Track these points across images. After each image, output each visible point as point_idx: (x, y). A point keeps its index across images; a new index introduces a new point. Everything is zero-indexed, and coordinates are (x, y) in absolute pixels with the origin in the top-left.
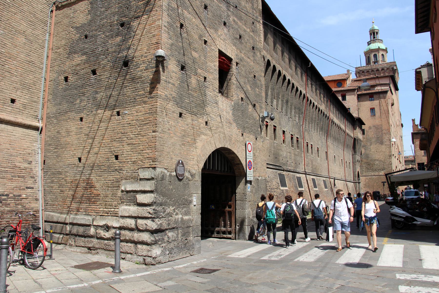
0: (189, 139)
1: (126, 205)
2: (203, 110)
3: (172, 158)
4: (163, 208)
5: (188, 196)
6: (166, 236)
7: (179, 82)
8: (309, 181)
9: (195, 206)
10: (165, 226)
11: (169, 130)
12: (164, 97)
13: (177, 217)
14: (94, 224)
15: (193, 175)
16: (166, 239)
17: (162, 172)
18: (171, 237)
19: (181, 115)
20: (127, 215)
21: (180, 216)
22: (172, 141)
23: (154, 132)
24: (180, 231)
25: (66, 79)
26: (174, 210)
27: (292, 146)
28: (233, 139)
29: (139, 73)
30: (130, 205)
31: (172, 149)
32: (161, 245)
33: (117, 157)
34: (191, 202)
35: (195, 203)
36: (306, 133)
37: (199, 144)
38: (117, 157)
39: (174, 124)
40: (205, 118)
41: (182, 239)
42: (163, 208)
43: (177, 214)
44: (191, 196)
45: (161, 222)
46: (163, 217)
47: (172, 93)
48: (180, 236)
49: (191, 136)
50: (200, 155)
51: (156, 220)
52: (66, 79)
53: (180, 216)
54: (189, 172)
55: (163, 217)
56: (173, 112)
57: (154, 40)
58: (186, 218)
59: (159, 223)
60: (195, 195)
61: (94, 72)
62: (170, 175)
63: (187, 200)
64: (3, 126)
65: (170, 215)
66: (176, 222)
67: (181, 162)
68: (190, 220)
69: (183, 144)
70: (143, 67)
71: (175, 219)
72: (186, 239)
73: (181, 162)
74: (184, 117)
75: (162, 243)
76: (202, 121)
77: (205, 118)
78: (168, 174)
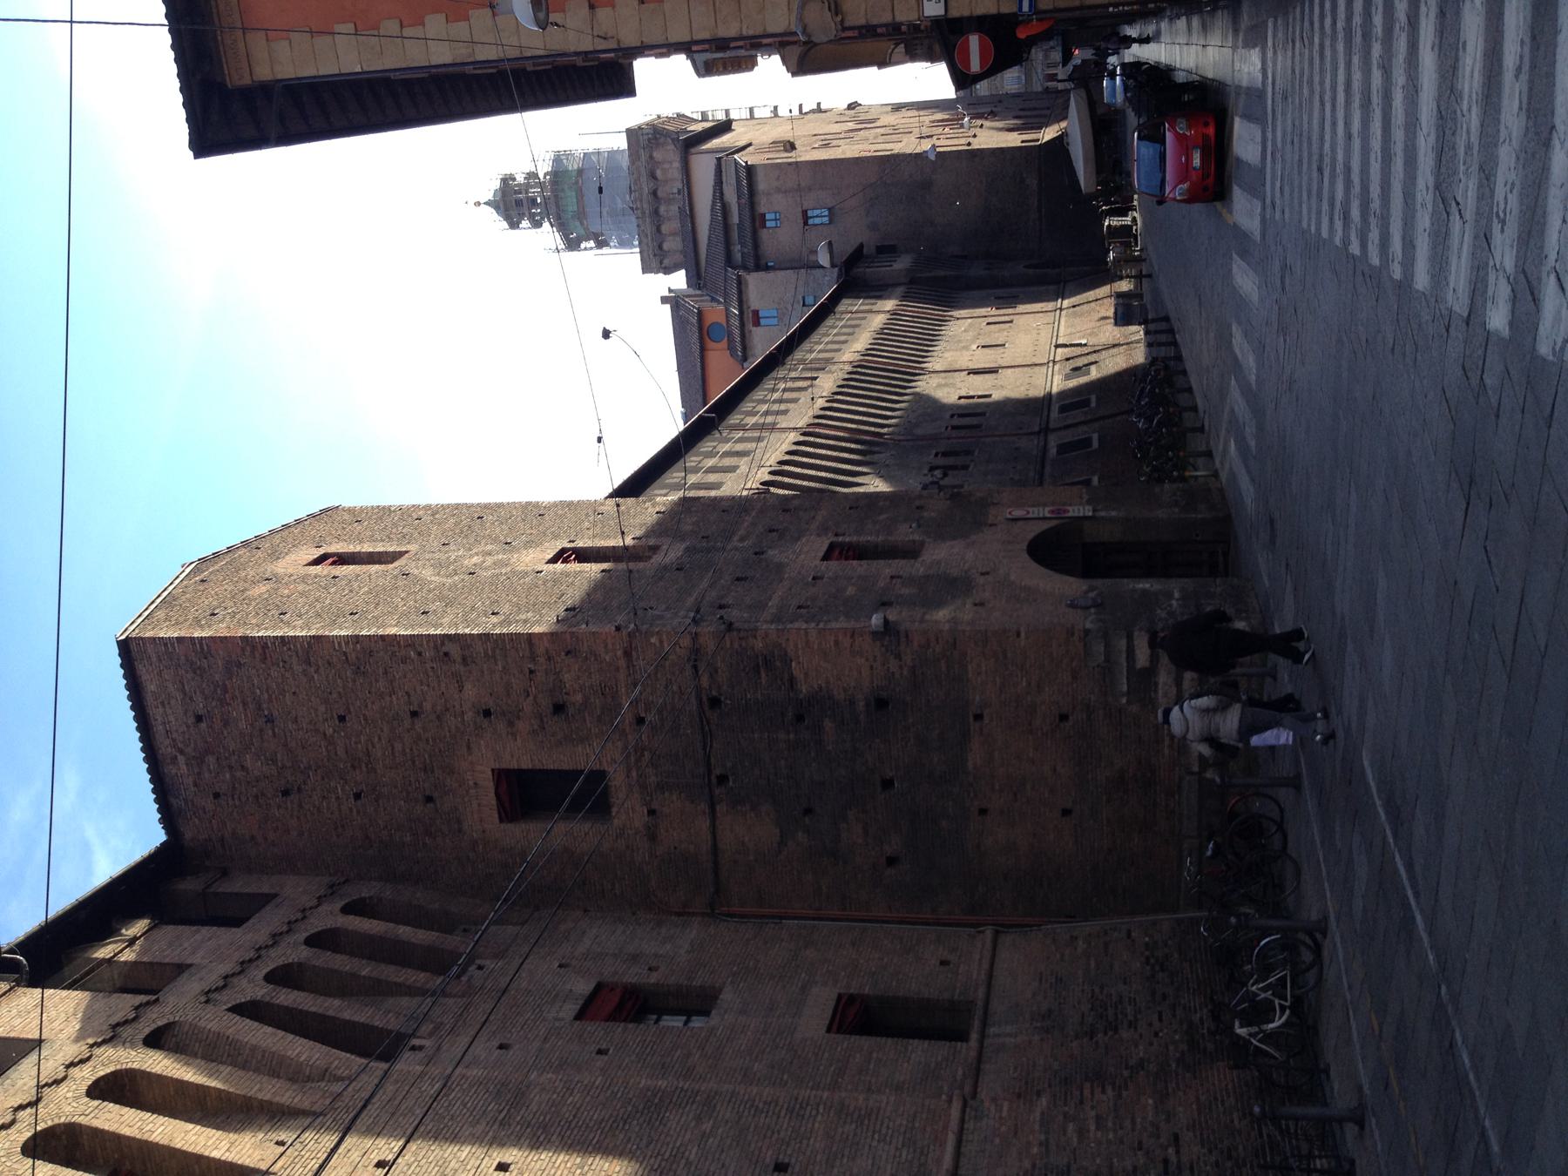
1: (1156, 691)
8: (1070, 422)
14: (1196, 769)
15: (1091, 589)
20: (1174, 690)
23: (1018, 635)
25: (891, 861)
27: (965, 467)
29: (905, 672)
30: (1156, 684)
33: (1064, 717)
36: (919, 432)
38: (1064, 717)
52: (891, 861)
57: (846, 642)
58: (1177, 595)
61: (887, 784)
64: (962, 1172)
70: (893, 665)
76: (981, 580)
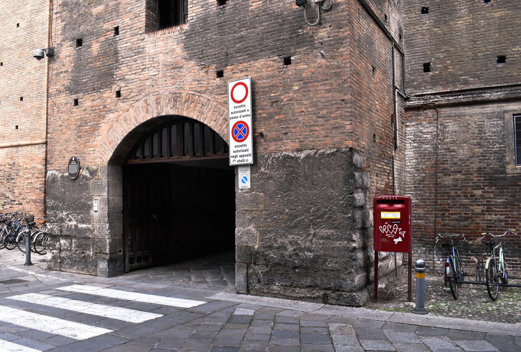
0: (87, 127)
2: (113, 77)
3: (64, 157)
4: (55, 212)
5: (86, 199)
6: (58, 243)
9: (96, 211)
10: (56, 231)
12: (55, 93)
13: (70, 223)
15: (93, 173)
16: (57, 245)
17: (52, 174)
18: (63, 244)
19: (76, 102)
21: (74, 223)
22: (64, 138)
24: (73, 240)
26: (67, 215)
28: (184, 95)
31: (64, 146)
32: (53, 251)
34: (90, 207)
37: (104, 127)
40: (115, 88)
41: (77, 250)
42: (55, 212)
43: (70, 220)
44: (91, 200)
45: (52, 226)
46: (54, 222)
48: (73, 245)
50: (105, 143)
53: (74, 223)
54: (87, 169)
56: (67, 103)
58: (80, 226)
59: (49, 227)
60: (98, 198)
62: (62, 177)
63: (84, 205)
65: (62, 220)
66: (69, 228)
67: (73, 159)
68: (88, 229)
69: (80, 137)
71: (68, 226)
72: (83, 253)
73: (73, 159)
74: (80, 102)
75: (53, 249)
77: (115, 88)
78: (60, 175)
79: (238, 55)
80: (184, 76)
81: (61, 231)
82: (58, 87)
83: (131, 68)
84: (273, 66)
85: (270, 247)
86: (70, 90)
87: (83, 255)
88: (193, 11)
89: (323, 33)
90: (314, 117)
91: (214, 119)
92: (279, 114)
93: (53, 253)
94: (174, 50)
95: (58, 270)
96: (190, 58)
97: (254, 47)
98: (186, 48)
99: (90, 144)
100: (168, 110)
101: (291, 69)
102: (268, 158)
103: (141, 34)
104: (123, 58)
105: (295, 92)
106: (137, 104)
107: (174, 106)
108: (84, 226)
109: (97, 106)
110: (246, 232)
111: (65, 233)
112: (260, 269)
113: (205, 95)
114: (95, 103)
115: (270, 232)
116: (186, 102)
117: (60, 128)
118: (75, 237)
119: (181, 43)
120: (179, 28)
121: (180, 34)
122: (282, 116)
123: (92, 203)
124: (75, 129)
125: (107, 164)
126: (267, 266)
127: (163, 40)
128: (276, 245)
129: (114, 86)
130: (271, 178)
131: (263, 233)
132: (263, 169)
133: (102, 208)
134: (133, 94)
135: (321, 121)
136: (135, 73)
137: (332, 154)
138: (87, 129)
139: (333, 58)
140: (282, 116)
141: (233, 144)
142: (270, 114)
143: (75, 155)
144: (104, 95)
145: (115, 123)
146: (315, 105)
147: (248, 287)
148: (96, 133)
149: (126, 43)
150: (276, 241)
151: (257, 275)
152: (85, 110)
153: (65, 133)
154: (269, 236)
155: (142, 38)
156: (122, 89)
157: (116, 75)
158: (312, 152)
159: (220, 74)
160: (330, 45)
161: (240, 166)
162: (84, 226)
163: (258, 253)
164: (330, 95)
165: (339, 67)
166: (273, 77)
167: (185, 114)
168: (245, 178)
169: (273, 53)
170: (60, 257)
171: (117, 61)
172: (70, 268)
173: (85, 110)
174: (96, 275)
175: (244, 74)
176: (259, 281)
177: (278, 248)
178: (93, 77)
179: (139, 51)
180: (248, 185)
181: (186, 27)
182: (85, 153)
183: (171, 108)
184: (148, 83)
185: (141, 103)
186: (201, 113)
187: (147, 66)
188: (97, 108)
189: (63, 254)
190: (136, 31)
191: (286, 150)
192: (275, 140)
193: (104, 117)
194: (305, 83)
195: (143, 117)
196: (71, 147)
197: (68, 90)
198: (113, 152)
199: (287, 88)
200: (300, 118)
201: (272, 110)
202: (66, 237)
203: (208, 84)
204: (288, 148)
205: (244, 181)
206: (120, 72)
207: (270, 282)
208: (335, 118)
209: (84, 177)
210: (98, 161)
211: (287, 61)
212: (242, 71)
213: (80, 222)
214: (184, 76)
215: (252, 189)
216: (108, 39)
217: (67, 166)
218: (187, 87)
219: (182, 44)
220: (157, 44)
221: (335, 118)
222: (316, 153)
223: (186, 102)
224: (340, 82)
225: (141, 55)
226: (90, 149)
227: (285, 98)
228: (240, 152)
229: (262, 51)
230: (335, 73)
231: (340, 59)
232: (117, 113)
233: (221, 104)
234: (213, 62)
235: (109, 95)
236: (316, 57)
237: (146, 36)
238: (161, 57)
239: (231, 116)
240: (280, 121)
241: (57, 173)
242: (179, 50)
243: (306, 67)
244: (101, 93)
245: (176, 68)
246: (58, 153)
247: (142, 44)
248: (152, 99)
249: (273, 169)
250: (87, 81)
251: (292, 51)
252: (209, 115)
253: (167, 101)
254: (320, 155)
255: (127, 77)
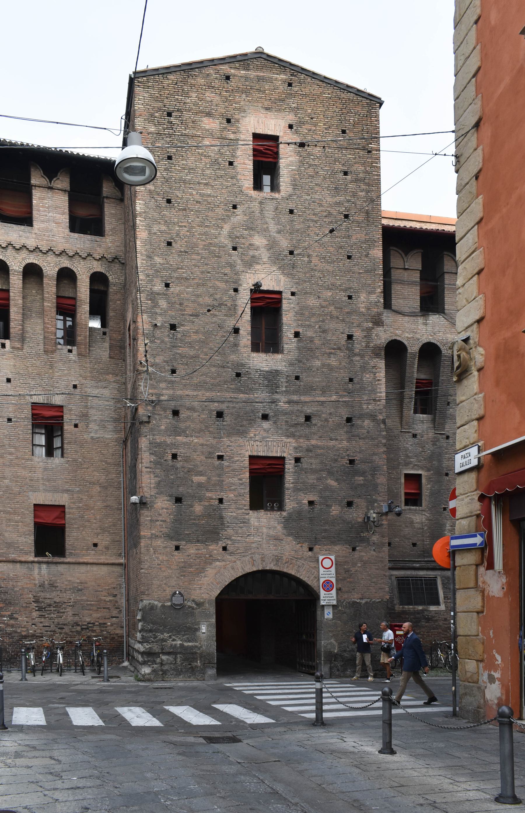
2: (219, 535)
7: (172, 517)
9: (203, 633)
11: (158, 565)
12: (149, 536)
13: (174, 643)
15: (199, 604)
19: (177, 548)
21: (179, 642)
22: (164, 574)
24: (178, 656)
26: (170, 636)
28: (284, 558)
34: (198, 629)
35: (204, 631)
37: (210, 571)
39: (165, 558)
40: (221, 544)
44: (198, 624)
46: (153, 642)
47: (162, 530)
48: (179, 660)
49: (196, 565)
50: (212, 583)
51: (145, 644)
54: (193, 601)
55: (153, 642)
60: (205, 623)
62: (163, 606)
63: (190, 628)
67: (177, 592)
68: (196, 647)
72: (190, 664)
73: (177, 592)
77: (221, 544)
78: (160, 604)
79: (323, 540)
80: (284, 546)
81: (162, 649)
82: (153, 532)
83: (237, 532)
84: (345, 551)
85: (345, 651)
86: (169, 537)
87: (190, 666)
88: (290, 504)
89: (375, 538)
90: (369, 582)
91: (307, 576)
92: (350, 578)
93: (153, 667)
94: (275, 527)
95: (161, 679)
96: (289, 535)
97: (334, 537)
98: (285, 528)
99: (195, 582)
100: (271, 566)
101: (357, 554)
102: (343, 602)
103: (245, 509)
104: (228, 523)
105: (359, 567)
106: (244, 559)
107: (276, 564)
108: (190, 644)
109: (202, 554)
110: (327, 642)
111: (167, 650)
112: (339, 664)
113: (300, 561)
114: (200, 552)
115: (344, 643)
116: (286, 563)
117: (158, 567)
118: (180, 653)
119: (281, 523)
120: (279, 513)
121: (280, 517)
122: (351, 580)
123: (199, 627)
124: (177, 569)
125: (214, 599)
126: (343, 661)
127: (266, 518)
128: (348, 650)
129: (220, 543)
130: (345, 613)
131: (340, 644)
132: (340, 608)
133: (210, 631)
134: (239, 551)
135: (373, 584)
136: (241, 537)
137: (379, 602)
138: (192, 570)
139: (379, 552)
140: (351, 580)
141: (322, 593)
142: (345, 577)
143: (179, 590)
144: (210, 547)
145: (222, 569)
146: (370, 576)
147: (331, 674)
148: (203, 575)
149: (232, 513)
150: (348, 647)
151: (337, 667)
152: (188, 556)
153: (165, 571)
154: (344, 645)
155: (247, 512)
156: (229, 545)
157: (222, 534)
158: (369, 600)
159: (311, 549)
160: (378, 545)
161: (326, 605)
162: (190, 644)
163: (337, 654)
164: (377, 571)
165: (383, 558)
166: (346, 557)
167: (285, 570)
168: (329, 612)
169: (346, 543)
170: (162, 670)
171: (223, 524)
172: (175, 677)
173: (188, 556)
174: (204, 680)
175: (328, 552)
176: (338, 670)
177: (349, 651)
178: (196, 531)
179: (246, 522)
180: (331, 616)
181: (284, 514)
182: (190, 589)
183: (274, 565)
184: (253, 545)
185: (247, 558)
186: (298, 572)
187: (252, 534)
188: (203, 556)
189: (166, 667)
190: (240, 506)
191: (354, 598)
192: (347, 592)
193: (211, 564)
194: (365, 563)
195: (249, 569)
196: (173, 582)
197: (167, 537)
198: (221, 590)
199: (354, 565)
200: (362, 582)
201: (345, 576)
202: (168, 654)
203: (303, 554)
204: (355, 597)
205: (328, 614)
206: (225, 533)
207: (346, 670)
208: (380, 584)
209: (190, 607)
210: (205, 596)
211: (354, 549)
212: (326, 550)
213: (186, 641)
214: (284, 546)
215: (333, 619)
216: (211, 505)
217: (169, 597)
218: (287, 554)
219: (282, 525)
220: (261, 520)
221: (380, 584)
222: (370, 601)
223: (286, 563)
224: (383, 565)
225: (247, 525)
226: (195, 586)
227: (353, 570)
228: (327, 598)
229: (339, 541)
230: (381, 561)
231: (383, 553)
232: (224, 563)
233: (312, 567)
234: (306, 541)
235: (215, 548)
236: (370, 550)
237: (251, 512)
238: (265, 530)
239: (321, 576)
240: (351, 582)
241: (156, 603)
242: (279, 527)
243: (365, 554)
244: (207, 545)
245: (277, 539)
246: (155, 586)
247: (247, 517)
248: (257, 557)
249: (346, 608)
250: (190, 534)
251: (357, 544)
252: (304, 573)
253: (271, 560)
254: (373, 602)
255: (233, 538)
